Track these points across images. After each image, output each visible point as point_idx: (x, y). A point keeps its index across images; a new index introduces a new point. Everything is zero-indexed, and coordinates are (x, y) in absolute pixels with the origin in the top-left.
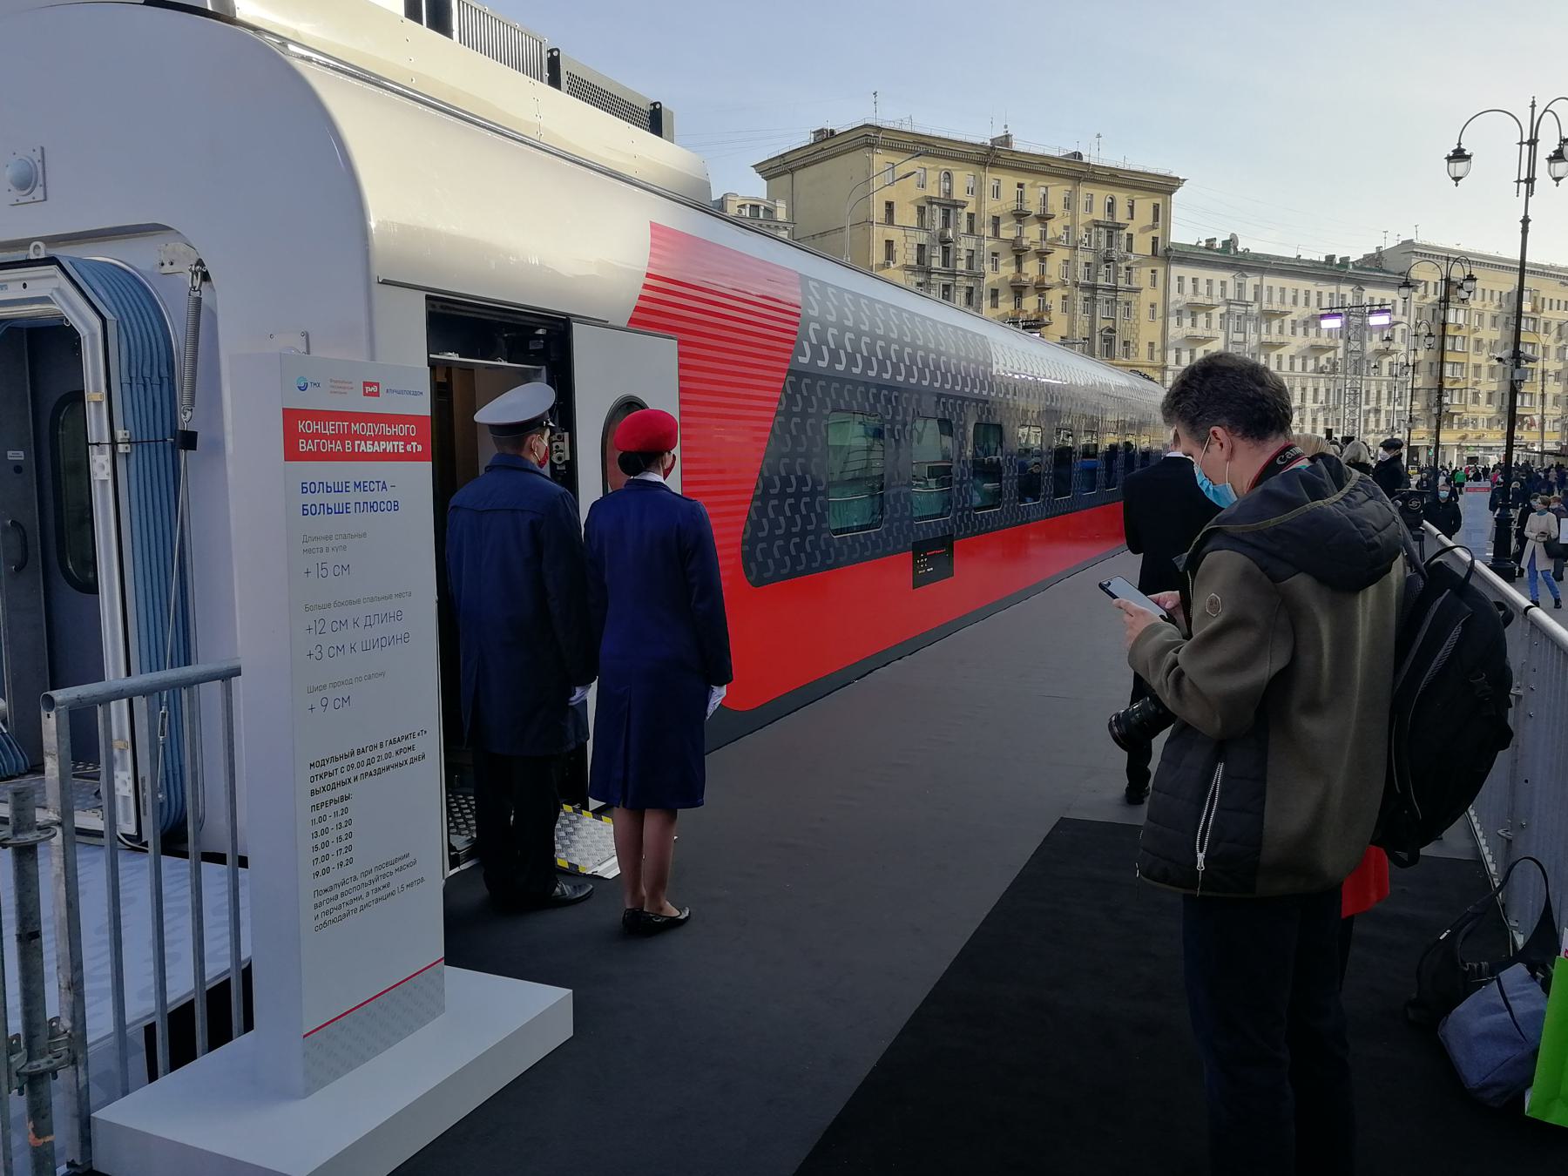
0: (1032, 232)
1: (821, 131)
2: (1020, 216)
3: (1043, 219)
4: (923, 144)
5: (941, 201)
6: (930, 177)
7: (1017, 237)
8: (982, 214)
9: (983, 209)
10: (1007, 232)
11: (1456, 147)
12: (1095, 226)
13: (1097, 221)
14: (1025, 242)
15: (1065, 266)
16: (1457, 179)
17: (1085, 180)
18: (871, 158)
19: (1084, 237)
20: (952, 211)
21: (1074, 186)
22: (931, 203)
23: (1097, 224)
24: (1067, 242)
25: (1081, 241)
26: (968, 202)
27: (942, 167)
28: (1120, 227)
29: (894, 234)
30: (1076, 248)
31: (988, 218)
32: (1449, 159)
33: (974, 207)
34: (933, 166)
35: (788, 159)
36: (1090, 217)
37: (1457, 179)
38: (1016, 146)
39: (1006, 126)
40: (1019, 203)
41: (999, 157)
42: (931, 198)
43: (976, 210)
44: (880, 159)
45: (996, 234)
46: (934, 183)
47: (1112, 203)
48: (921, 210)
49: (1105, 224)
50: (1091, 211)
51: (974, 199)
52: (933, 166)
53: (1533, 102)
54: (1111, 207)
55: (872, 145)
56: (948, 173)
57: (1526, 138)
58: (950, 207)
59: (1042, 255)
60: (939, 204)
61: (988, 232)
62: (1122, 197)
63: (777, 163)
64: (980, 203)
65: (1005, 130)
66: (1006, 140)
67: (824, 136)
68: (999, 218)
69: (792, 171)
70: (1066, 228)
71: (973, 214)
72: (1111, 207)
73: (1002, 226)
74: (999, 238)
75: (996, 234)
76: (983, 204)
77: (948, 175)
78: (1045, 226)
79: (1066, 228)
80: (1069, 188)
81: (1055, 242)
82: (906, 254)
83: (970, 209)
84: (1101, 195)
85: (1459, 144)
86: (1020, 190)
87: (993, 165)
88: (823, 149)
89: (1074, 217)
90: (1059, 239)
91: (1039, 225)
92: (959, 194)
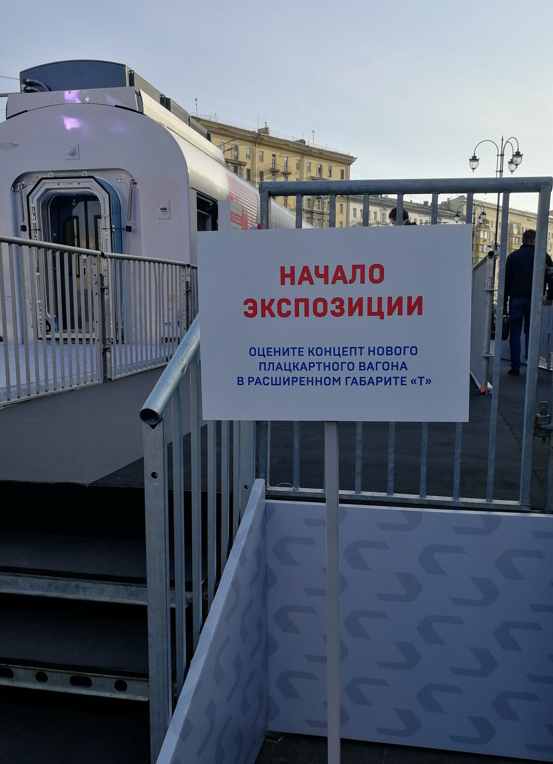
2: (274, 172)
4: (223, 129)
8: (254, 170)
9: (254, 167)
11: (473, 155)
13: (313, 177)
16: (473, 169)
17: (308, 155)
20: (239, 167)
21: (301, 158)
26: (247, 163)
31: (257, 172)
32: (470, 160)
33: (250, 166)
36: (309, 175)
37: (473, 169)
38: (272, 134)
39: (266, 123)
40: (273, 165)
41: (263, 139)
43: (251, 167)
47: (321, 168)
50: (310, 171)
53: (503, 138)
54: (320, 170)
56: (236, 146)
57: (500, 153)
60: (232, 163)
62: (325, 165)
64: (253, 164)
65: (265, 125)
66: (266, 130)
68: (263, 172)
71: (250, 170)
72: (320, 170)
73: (265, 177)
76: (255, 165)
80: (299, 159)
83: (248, 166)
84: (315, 163)
85: (474, 154)
86: (274, 158)
87: (259, 144)
92: (242, 158)
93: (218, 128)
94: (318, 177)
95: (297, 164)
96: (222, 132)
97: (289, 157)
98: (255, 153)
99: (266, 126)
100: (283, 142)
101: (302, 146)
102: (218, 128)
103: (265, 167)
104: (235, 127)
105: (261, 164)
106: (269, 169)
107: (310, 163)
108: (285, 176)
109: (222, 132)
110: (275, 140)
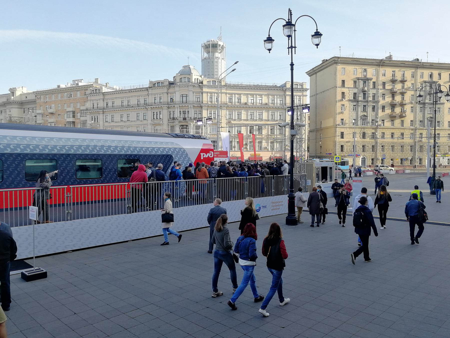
0: (398, 87)
1: (324, 60)
2: (393, 81)
3: (403, 82)
5: (362, 79)
6: (359, 72)
7: (392, 88)
8: (379, 81)
9: (379, 80)
10: (388, 87)
12: (425, 83)
14: (395, 90)
15: (412, 97)
17: (420, 68)
18: (336, 67)
19: (420, 87)
20: (367, 82)
21: (416, 70)
22: (359, 79)
23: (425, 82)
24: (413, 89)
25: (418, 88)
26: (373, 78)
27: (363, 67)
28: (434, 82)
29: (344, 90)
30: (416, 90)
31: (380, 83)
33: (375, 80)
34: (360, 67)
35: (315, 69)
36: (422, 80)
38: (394, 59)
39: (390, 53)
40: (393, 77)
41: (385, 63)
42: (358, 78)
44: (339, 67)
45: (384, 87)
46: (360, 73)
48: (355, 82)
49: (428, 82)
50: (423, 78)
51: (375, 77)
52: (360, 67)
54: (431, 76)
55: (337, 63)
58: (366, 80)
59: (403, 94)
60: (362, 80)
61: (381, 87)
62: (436, 73)
63: (311, 71)
64: (378, 78)
65: (390, 54)
66: (390, 57)
67: (324, 61)
69: (316, 73)
70: (412, 84)
71: (375, 82)
72: (431, 76)
73: (386, 85)
74: (385, 89)
75: (384, 87)
77: (365, 70)
78: (404, 84)
79: (412, 84)
80: (414, 71)
81: (408, 89)
82: (349, 95)
83: (374, 80)
84: (427, 73)
86: (393, 73)
87: (382, 65)
88: (323, 66)
89: (416, 80)
90: (409, 88)
91: (401, 84)
93: (352, 61)
94: (429, 80)
95: (412, 75)
96: (355, 62)
97: (406, 71)
98: (379, 71)
99: (391, 54)
100: (400, 62)
101: (415, 63)
102: (352, 61)
103: (387, 79)
104: (371, 59)
105: (384, 78)
106: (390, 80)
107: (423, 72)
108: (402, 83)
109: (355, 62)
110: (394, 62)
